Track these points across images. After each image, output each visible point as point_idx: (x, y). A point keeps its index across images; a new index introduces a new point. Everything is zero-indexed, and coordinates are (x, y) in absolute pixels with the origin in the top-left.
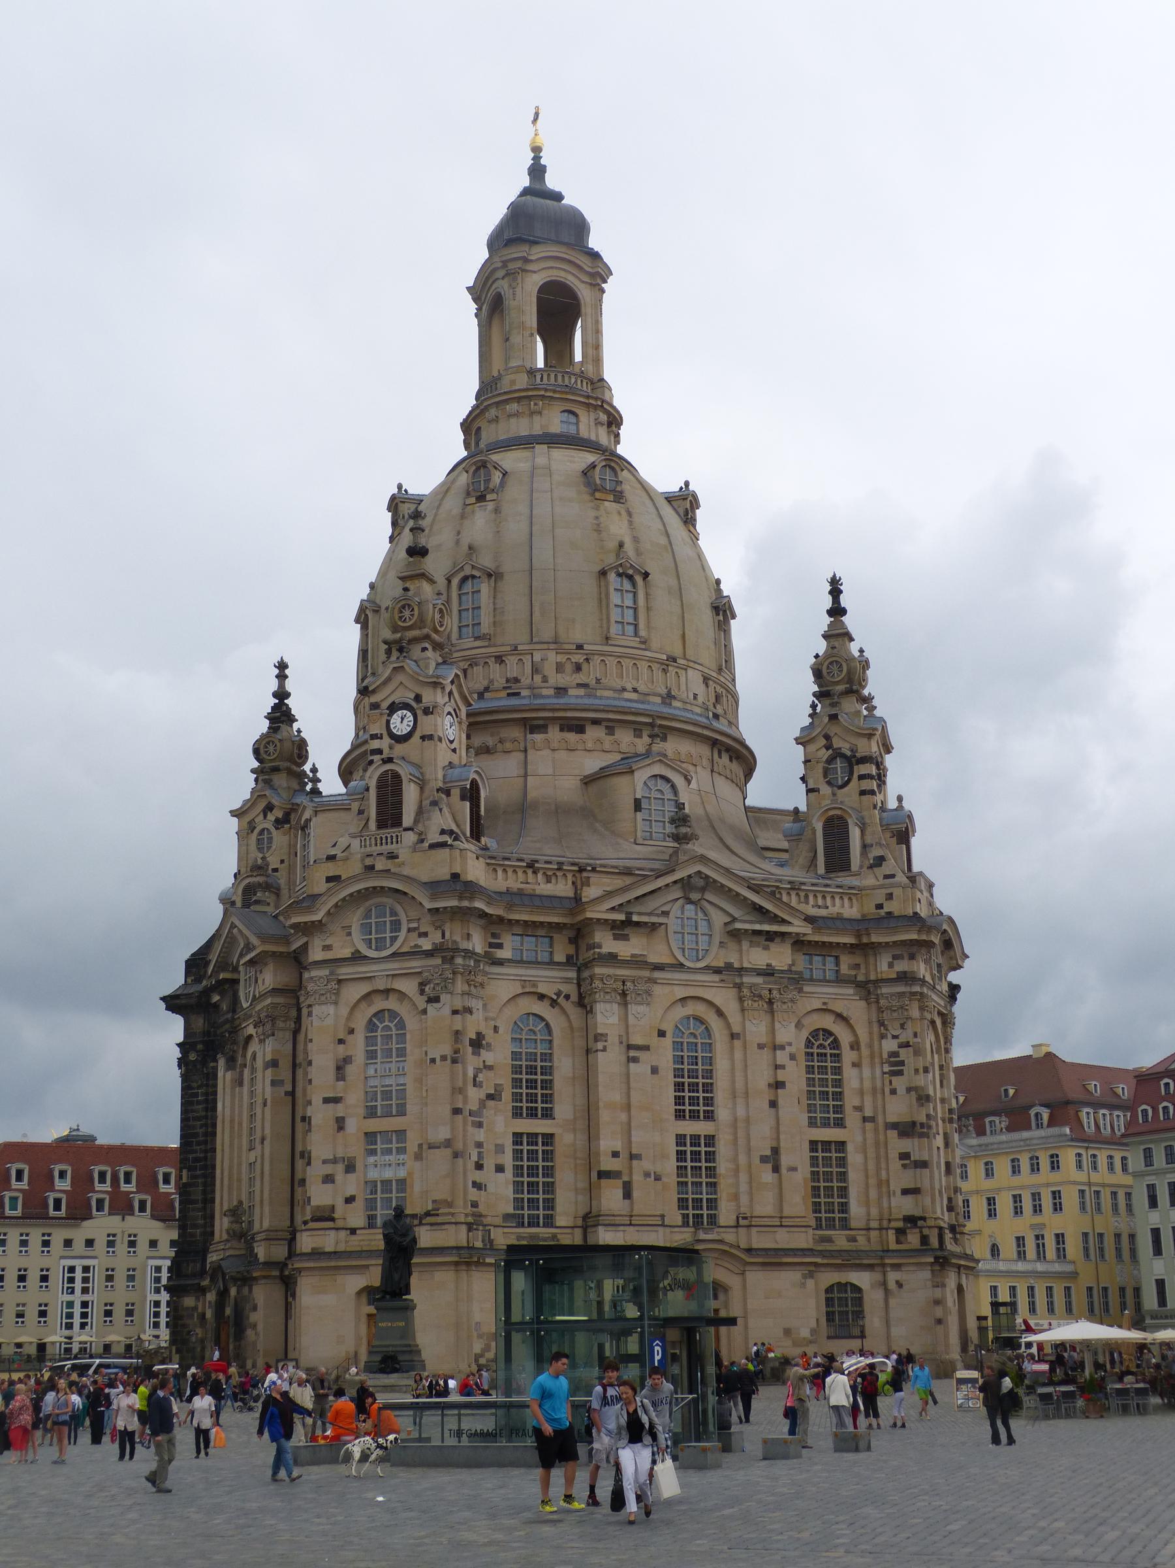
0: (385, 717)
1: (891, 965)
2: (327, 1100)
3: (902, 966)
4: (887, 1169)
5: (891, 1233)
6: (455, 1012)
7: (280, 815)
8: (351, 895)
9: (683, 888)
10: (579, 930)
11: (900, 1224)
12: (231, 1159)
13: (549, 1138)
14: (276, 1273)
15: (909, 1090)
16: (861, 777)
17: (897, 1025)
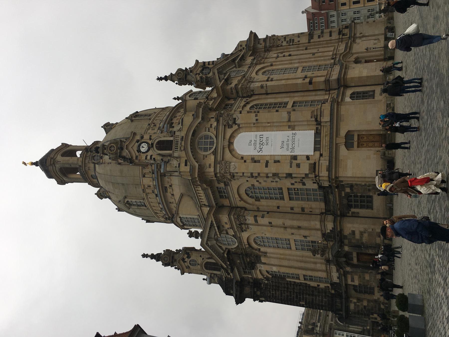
0: (141, 154)
1: (261, 44)
2: (267, 166)
3: (262, 42)
4: (324, 41)
5: (343, 37)
6: (241, 113)
7: (186, 256)
8: (192, 152)
9: (221, 74)
10: (226, 97)
11: (341, 35)
12: (294, 260)
13: (294, 103)
14: (339, 218)
15: (299, 37)
16: (209, 64)
17: (278, 42)
